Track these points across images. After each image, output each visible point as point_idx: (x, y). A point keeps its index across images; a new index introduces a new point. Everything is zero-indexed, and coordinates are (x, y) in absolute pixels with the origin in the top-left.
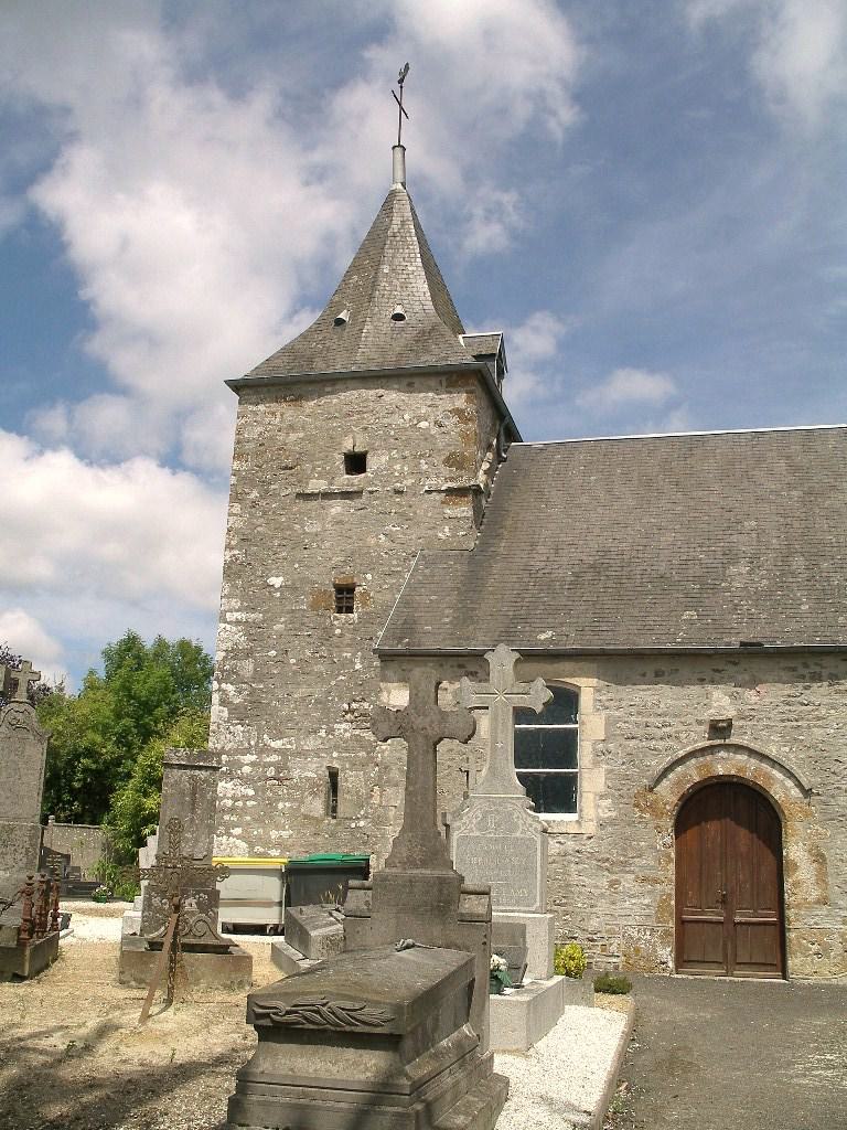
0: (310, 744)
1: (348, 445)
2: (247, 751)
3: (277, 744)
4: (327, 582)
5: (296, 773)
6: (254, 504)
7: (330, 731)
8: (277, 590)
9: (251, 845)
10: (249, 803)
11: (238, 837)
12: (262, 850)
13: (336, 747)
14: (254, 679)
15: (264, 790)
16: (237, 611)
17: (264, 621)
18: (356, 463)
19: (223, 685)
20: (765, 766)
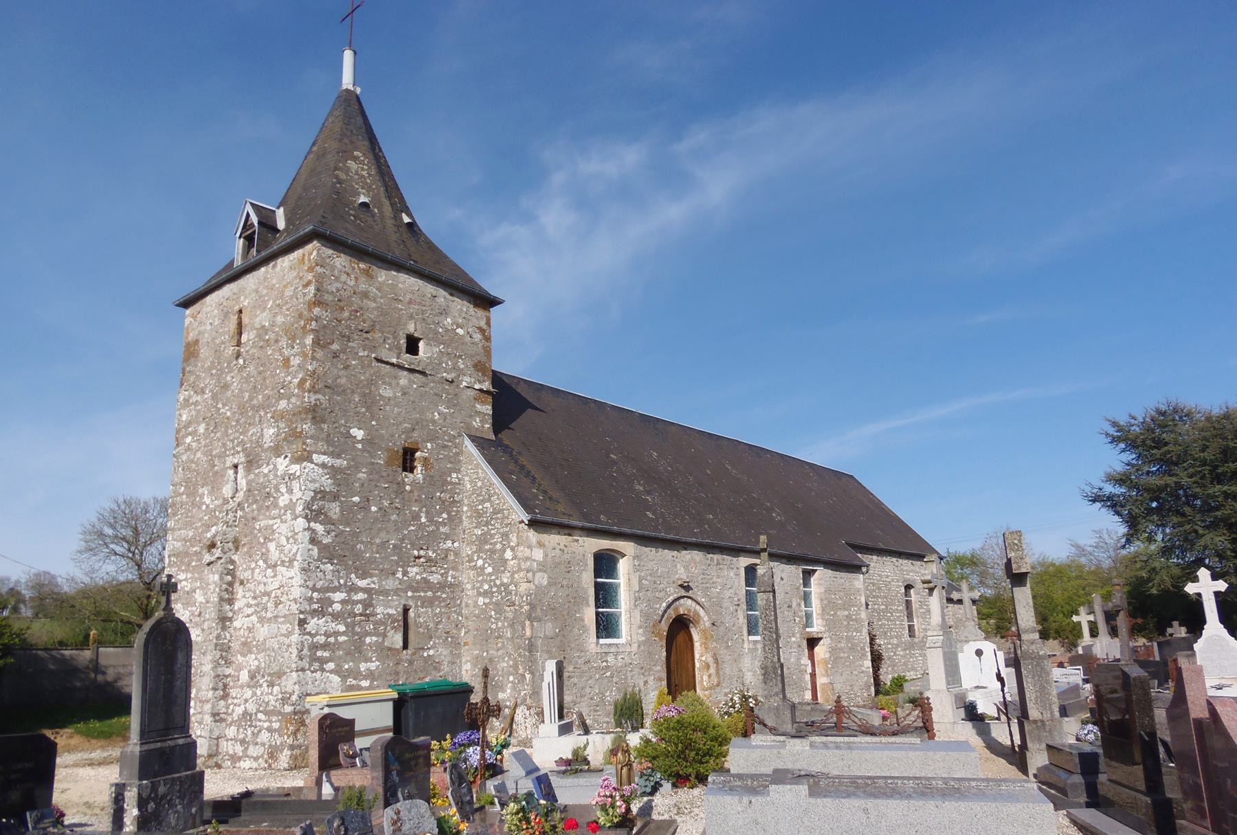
0: (390, 584)
1: (411, 328)
2: (334, 590)
3: (362, 583)
4: (400, 443)
5: (379, 610)
6: (335, 355)
7: (405, 573)
8: (359, 442)
9: (344, 678)
10: (342, 639)
11: (331, 672)
12: (354, 682)
13: (410, 588)
14: (340, 521)
15: (353, 624)
16: (324, 454)
17: (348, 468)
18: (412, 345)
19: (312, 524)
20: (698, 607)
